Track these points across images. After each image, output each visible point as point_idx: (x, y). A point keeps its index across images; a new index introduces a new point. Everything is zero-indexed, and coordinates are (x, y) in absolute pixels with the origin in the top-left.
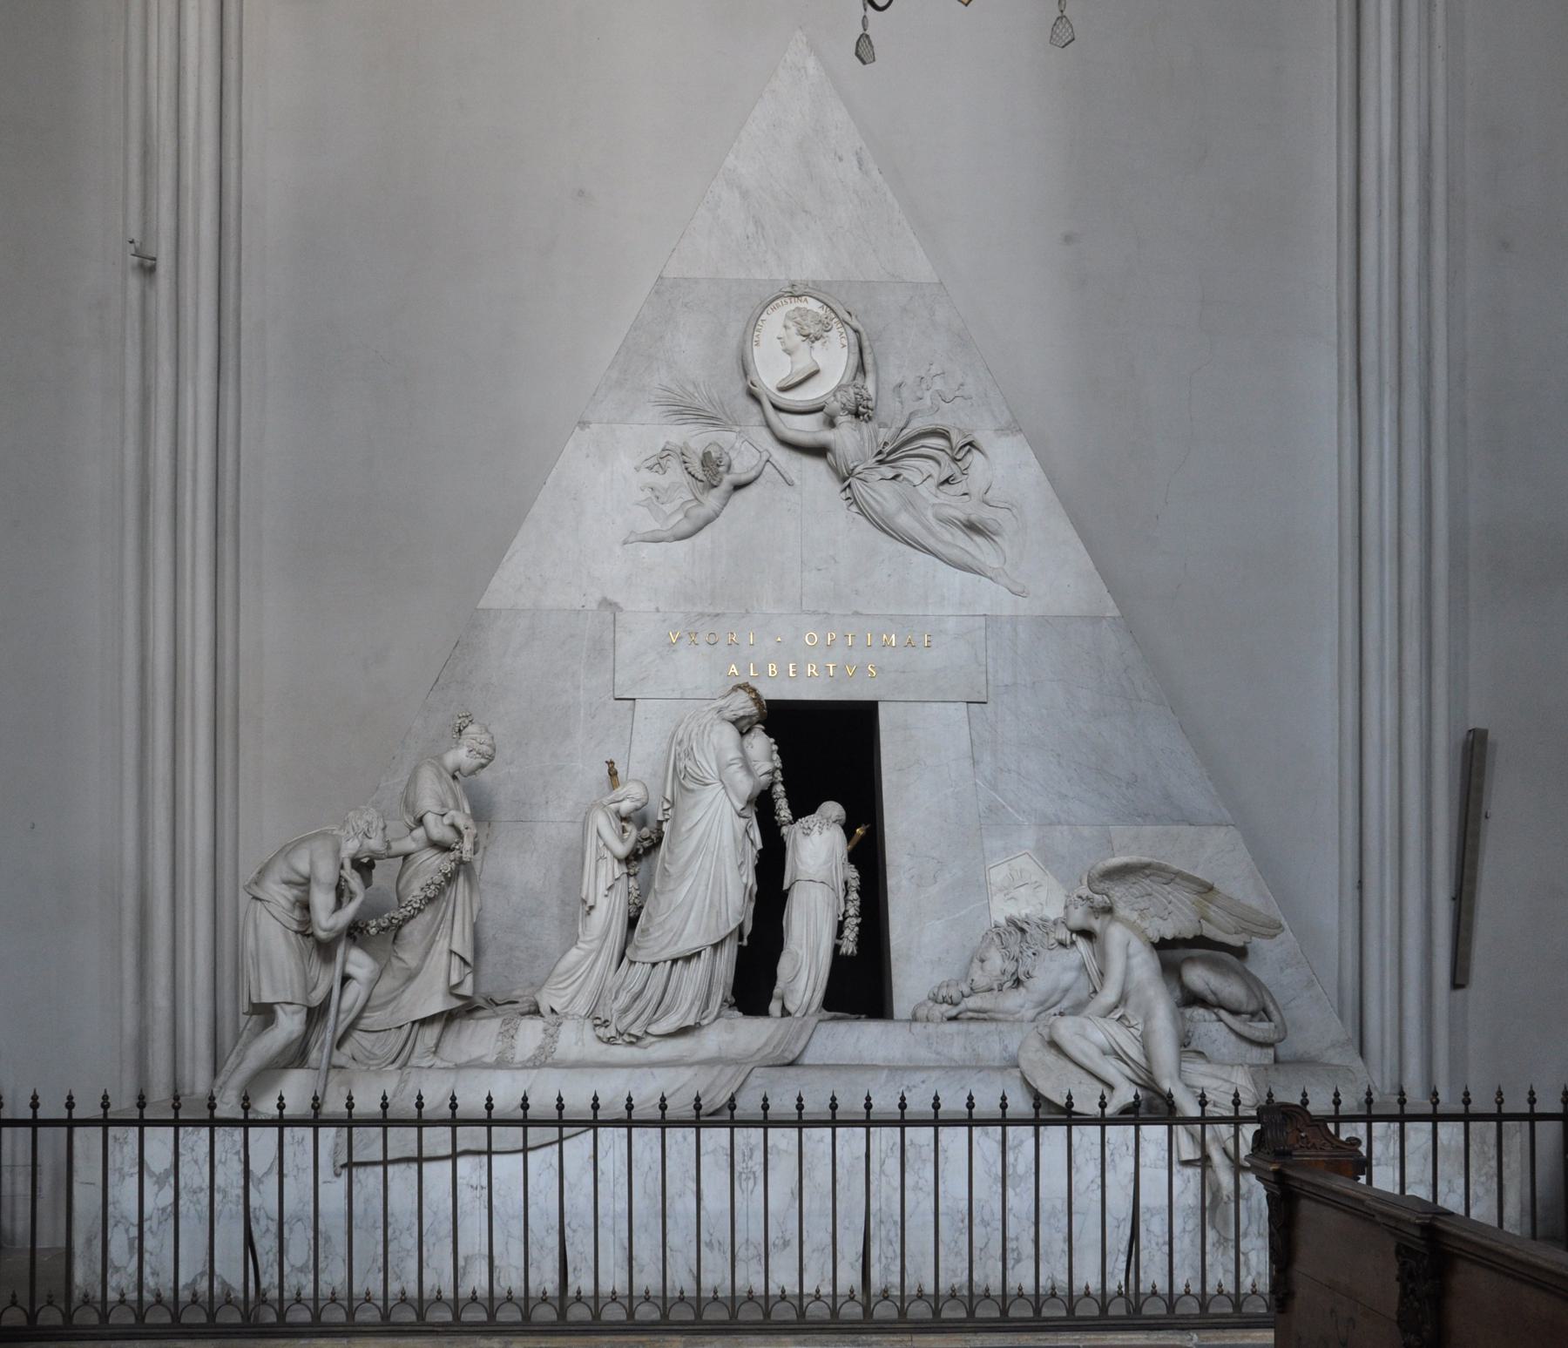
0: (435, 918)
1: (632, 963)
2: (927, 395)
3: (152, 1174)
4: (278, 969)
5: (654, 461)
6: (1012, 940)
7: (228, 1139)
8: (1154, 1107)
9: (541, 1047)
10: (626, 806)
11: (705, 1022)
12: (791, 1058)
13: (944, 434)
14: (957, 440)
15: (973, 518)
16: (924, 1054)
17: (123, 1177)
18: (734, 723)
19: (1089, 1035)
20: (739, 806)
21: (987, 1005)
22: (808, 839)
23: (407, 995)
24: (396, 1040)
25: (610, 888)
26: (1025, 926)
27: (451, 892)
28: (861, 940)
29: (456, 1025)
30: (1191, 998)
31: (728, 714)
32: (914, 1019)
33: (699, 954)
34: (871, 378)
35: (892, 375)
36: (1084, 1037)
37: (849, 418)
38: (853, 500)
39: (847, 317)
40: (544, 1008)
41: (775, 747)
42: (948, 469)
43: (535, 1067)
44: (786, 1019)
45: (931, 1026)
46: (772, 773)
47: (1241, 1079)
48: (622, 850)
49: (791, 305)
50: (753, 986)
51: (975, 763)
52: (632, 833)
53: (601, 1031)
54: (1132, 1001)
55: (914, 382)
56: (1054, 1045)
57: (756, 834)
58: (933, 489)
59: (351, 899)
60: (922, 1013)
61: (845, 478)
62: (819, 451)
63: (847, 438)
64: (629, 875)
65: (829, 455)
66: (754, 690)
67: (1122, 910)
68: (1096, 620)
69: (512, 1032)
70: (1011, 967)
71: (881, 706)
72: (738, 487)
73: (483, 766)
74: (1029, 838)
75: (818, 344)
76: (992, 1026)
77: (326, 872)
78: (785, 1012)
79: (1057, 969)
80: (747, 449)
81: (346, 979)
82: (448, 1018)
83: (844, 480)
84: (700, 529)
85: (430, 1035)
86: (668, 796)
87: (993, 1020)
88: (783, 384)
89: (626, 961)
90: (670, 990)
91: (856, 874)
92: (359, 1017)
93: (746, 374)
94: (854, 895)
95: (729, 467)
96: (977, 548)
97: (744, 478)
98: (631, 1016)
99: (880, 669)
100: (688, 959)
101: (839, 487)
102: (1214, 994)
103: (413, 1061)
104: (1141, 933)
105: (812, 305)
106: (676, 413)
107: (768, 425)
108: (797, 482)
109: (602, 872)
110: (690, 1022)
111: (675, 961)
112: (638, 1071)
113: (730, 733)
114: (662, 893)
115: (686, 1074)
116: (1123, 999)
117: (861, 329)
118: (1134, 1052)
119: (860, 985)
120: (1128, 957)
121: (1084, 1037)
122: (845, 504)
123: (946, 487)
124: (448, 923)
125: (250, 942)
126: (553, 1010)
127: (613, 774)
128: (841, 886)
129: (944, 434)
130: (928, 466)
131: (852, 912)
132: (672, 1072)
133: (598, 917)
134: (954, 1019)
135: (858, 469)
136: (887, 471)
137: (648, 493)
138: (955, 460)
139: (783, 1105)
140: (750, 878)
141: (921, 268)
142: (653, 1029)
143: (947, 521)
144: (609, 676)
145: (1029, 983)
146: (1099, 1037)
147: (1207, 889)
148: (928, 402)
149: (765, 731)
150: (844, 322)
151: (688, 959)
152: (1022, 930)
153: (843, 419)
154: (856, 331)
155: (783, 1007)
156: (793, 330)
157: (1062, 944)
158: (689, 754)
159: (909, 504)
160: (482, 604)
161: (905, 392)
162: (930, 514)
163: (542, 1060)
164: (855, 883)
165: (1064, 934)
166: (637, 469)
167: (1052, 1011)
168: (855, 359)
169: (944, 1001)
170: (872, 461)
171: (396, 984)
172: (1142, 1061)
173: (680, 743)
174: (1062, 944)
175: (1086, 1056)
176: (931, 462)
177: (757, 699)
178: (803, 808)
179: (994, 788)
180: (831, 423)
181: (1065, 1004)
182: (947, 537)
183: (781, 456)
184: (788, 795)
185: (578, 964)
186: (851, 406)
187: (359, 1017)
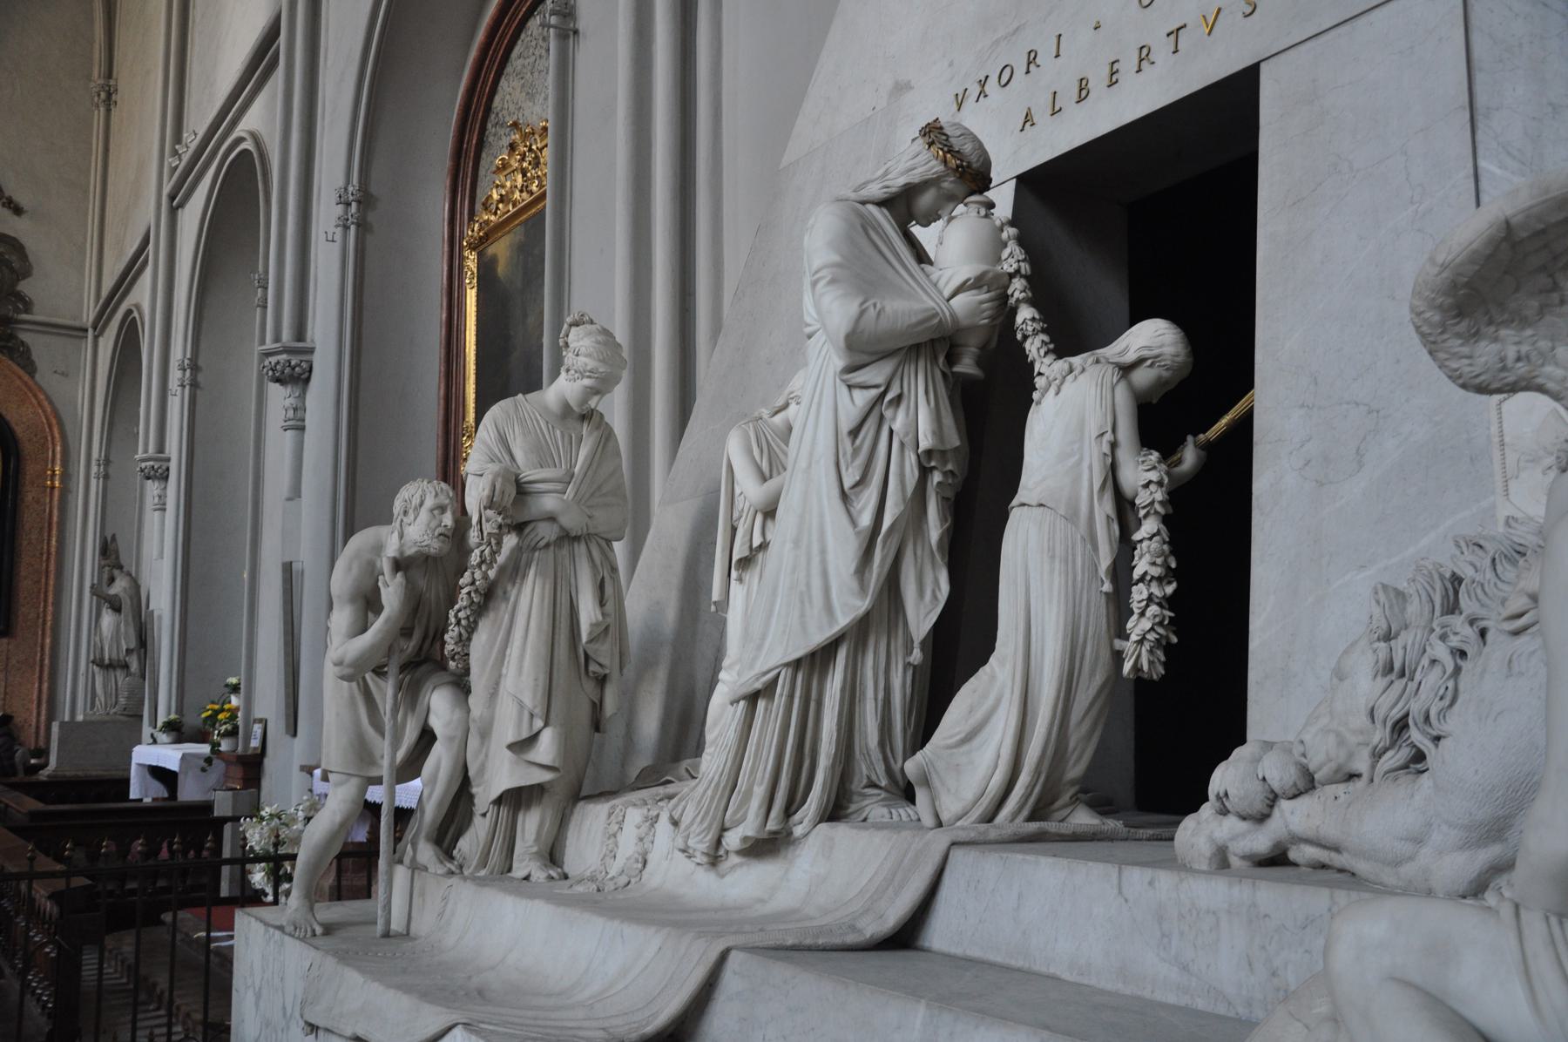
20: (839, 363)
81: (427, 737)
85: (531, 824)
128: (1105, 507)
134: (1276, 859)
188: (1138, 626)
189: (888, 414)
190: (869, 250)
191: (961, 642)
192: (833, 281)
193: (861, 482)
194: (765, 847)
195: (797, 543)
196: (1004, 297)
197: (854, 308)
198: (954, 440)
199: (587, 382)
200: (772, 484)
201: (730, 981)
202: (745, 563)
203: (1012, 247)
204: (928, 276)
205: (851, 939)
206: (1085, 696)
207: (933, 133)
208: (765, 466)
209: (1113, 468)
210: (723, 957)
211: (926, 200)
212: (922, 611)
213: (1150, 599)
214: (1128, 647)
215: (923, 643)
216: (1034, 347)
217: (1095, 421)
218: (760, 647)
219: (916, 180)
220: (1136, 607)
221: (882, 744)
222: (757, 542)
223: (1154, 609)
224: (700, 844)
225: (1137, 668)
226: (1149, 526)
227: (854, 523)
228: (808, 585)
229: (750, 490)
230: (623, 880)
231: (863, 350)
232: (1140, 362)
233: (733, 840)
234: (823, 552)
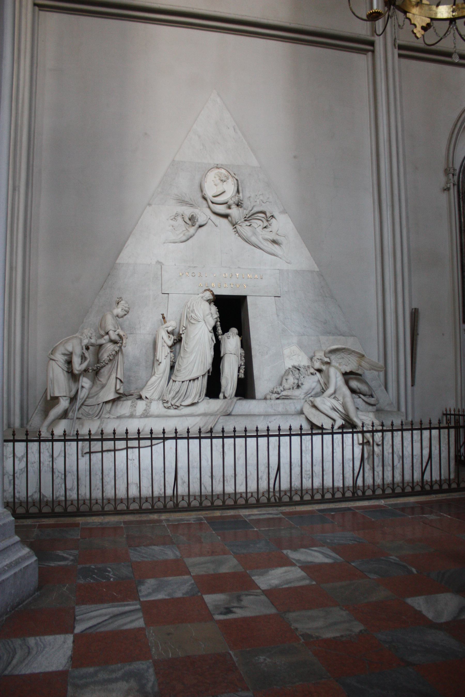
0: (112, 366)
1: (174, 381)
2: (258, 201)
3: (17, 457)
4: (60, 386)
5: (173, 217)
6: (296, 373)
7: (46, 446)
8: (349, 426)
9: (145, 410)
10: (170, 329)
11: (200, 401)
12: (229, 412)
13: (264, 213)
14: (268, 215)
15: (275, 239)
16: (271, 411)
17: (7, 459)
18: (207, 301)
19: (326, 403)
21: (289, 394)
22: (229, 340)
23: (101, 394)
24: (97, 409)
25: (166, 356)
26: (299, 368)
27: (116, 358)
28: (245, 373)
29: (116, 403)
30: (353, 391)
31: (205, 299)
32: (265, 399)
33: (198, 378)
34: (241, 195)
35: (247, 194)
36: (325, 404)
37: (236, 206)
38: (237, 232)
39: (234, 175)
40: (143, 397)
41: (217, 310)
42: (266, 224)
43: (144, 417)
44: (226, 400)
45: (272, 401)
46: (216, 318)
47: (371, 415)
48: (170, 343)
49: (217, 171)
50: (213, 389)
51: (278, 316)
52: (173, 338)
53: (165, 405)
54: (338, 392)
55: (254, 197)
56: (314, 407)
57: (214, 338)
58: (261, 230)
59: (85, 361)
60: (268, 397)
61: (234, 225)
62: (226, 216)
63: (235, 212)
64: (171, 352)
65: (229, 218)
66: (212, 291)
67: (334, 363)
68: (312, 272)
69: (135, 405)
70: (296, 381)
71: (248, 298)
72: (200, 226)
73: (125, 315)
74: (295, 340)
75: (225, 183)
76: (291, 401)
77: (78, 351)
78: (225, 397)
79: (311, 382)
80: (203, 214)
82: (113, 401)
83: (234, 226)
84: (188, 239)
85: (108, 406)
86: (185, 326)
87: (291, 399)
88: (214, 195)
89: (171, 381)
90: (189, 390)
91: (243, 352)
92: (85, 401)
93: (202, 191)
94: (243, 359)
95: (197, 220)
96: (275, 248)
97: (203, 223)
98: (176, 400)
99: (247, 285)
100: (194, 380)
101: (232, 228)
102: (359, 389)
103: (103, 416)
104: (340, 370)
105: (223, 171)
106: (179, 202)
107: (209, 207)
108: (219, 226)
109: (164, 350)
110: (196, 401)
111: (190, 381)
112: (182, 418)
113: (207, 304)
114: (184, 358)
115: (198, 419)
116: (335, 392)
117: (238, 179)
118: (341, 409)
119: (245, 389)
120: (336, 378)
121: (325, 404)
122: (234, 233)
123: (265, 229)
124: (116, 368)
125: (51, 375)
126: (146, 397)
127: (164, 318)
128: (239, 356)
129: (264, 213)
130: (260, 222)
131: (243, 364)
132: (193, 418)
133: (162, 367)
134: (278, 399)
135: (239, 222)
137: (171, 227)
138: (268, 221)
139: (229, 428)
140: (212, 353)
141: (254, 162)
142: (184, 404)
143: (267, 240)
144: (160, 286)
145: (303, 387)
146: (329, 404)
147: (362, 356)
148: (258, 202)
149: (214, 305)
150: (233, 177)
151: (194, 380)
152: (299, 370)
153: (234, 207)
154: (237, 180)
155: (224, 396)
156: (218, 178)
157: (312, 374)
158: (193, 311)
159: (254, 234)
160: (118, 261)
161: (251, 199)
162: (260, 237)
163: (146, 415)
164: (243, 354)
165: (312, 371)
166: (167, 219)
167: (309, 395)
168: (236, 188)
169: (276, 393)
170: (243, 220)
171: (98, 389)
172: (343, 411)
173: (189, 308)
174: (312, 374)
175: (326, 410)
176: (260, 221)
177: (213, 294)
178: (225, 330)
179: (284, 324)
180: (229, 207)
181: (313, 393)
182: (266, 244)
183: (213, 217)
184: (221, 326)
185: (155, 382)
186: (236, 202)
187: (85, 401)
199: (126, 313)
218: (192, 372)
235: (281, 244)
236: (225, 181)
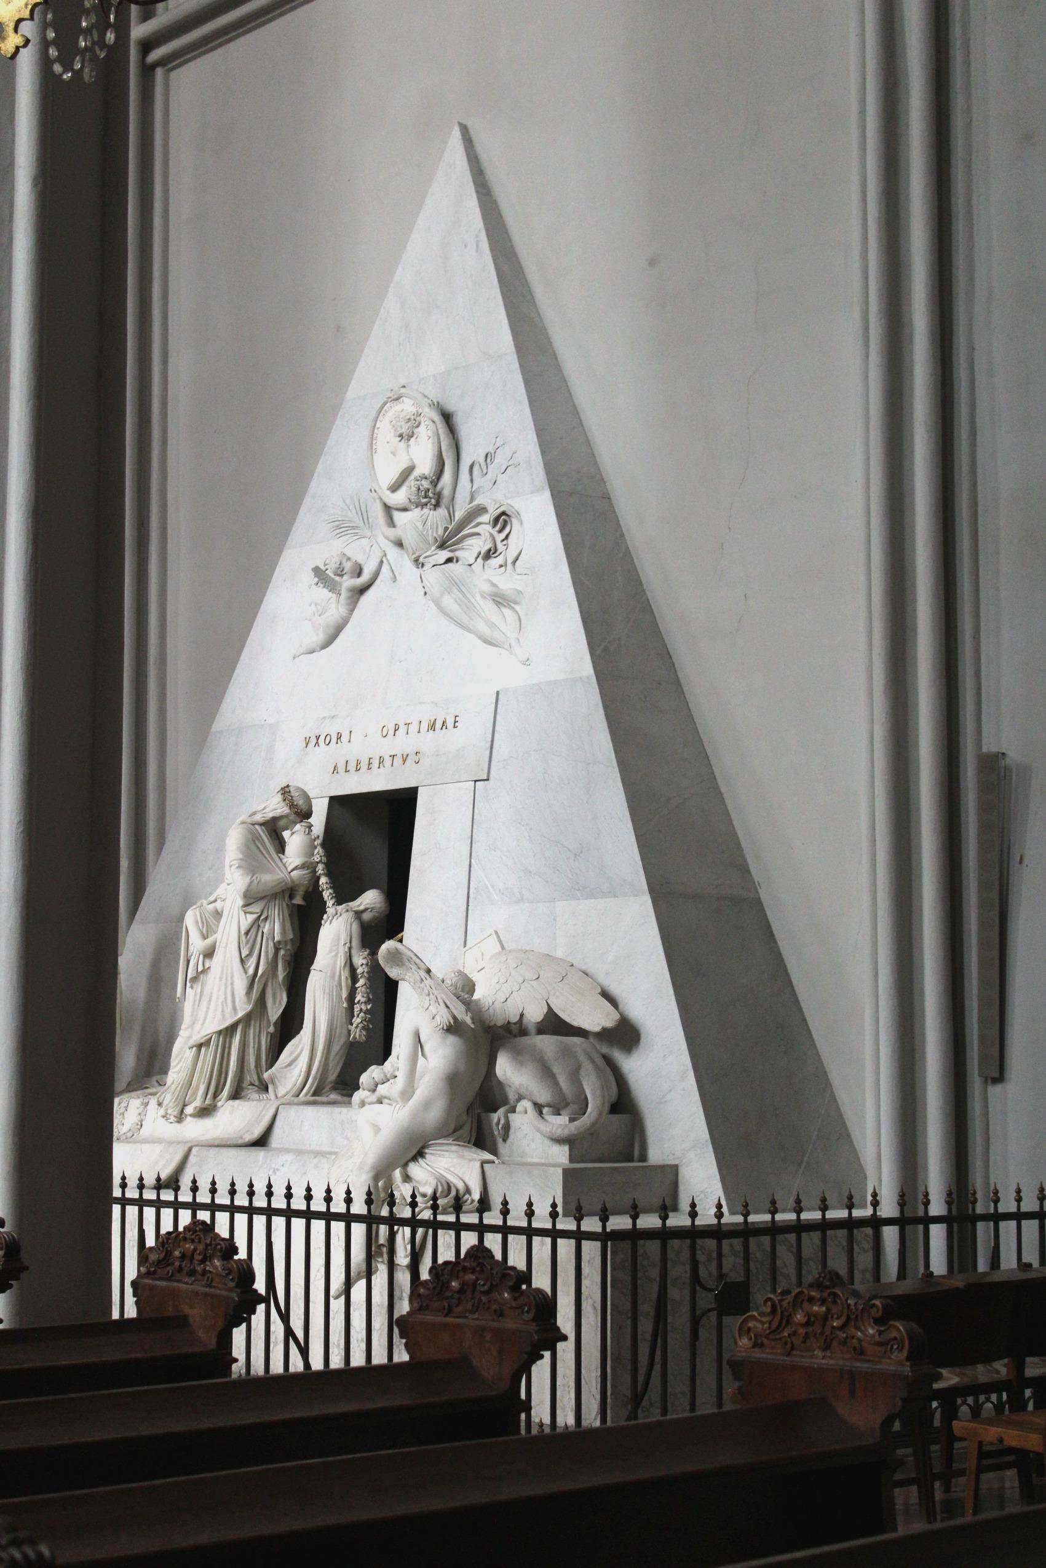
72: (363, 590)
128: (345, 974)
136: (445, 555)
184: (335, 885)
188: (357, 1021)
189: (262, 925)
190: (255, 849)
191: (290, 1024)
192: (239, 867)
193: (250, 955)
194: (205, 1112)
195: (221, 978)
196: (315, 872)
197: (248, 880)
198: (290, 936)
200: (209, 941)
201: (192, 1159)
202: (195, 979)
203: (319, 849)
204: (281, 860)
205: (240, 1142)
206: (336, 1048)
207: (285, 791)
208: (204, 931)
209: (350, 957)
210: (190, 1150)
211: (282, 823)
212: (276, 1008)
213: (361, 1010)
214: (353, 1028)
215: (275, 1024)
216: (326, 894)
217: (344, 937)
219: (278, 815)
220: (356, 1014)
221: (256, 1067)
222: (200, 969)
223: (362, 1014)
224: (173, 1112)
225: (354, 1037)
226: (361, 982)
227: (246, 972)
228: (226, 998)
229: (197, 944)
230: (130, 1134)
231: (250, 898)
232: (365, 910)
233: (189, 1110)
234: (232, 984)
235: (515, 603)
236: (410, 436)
